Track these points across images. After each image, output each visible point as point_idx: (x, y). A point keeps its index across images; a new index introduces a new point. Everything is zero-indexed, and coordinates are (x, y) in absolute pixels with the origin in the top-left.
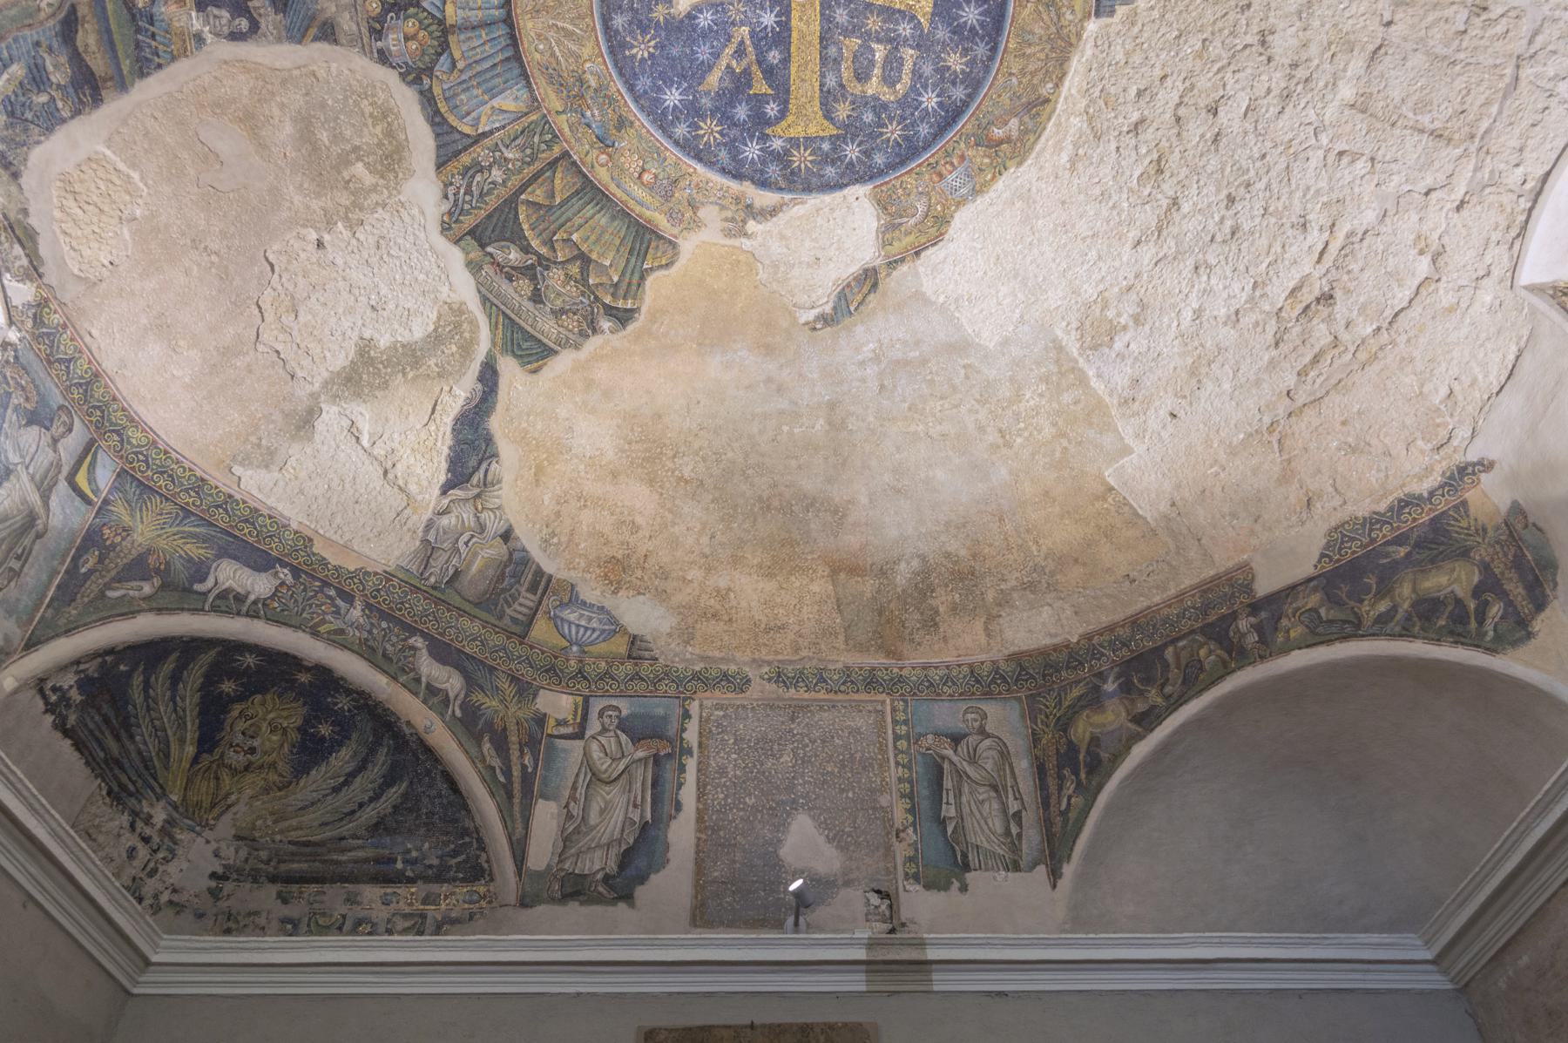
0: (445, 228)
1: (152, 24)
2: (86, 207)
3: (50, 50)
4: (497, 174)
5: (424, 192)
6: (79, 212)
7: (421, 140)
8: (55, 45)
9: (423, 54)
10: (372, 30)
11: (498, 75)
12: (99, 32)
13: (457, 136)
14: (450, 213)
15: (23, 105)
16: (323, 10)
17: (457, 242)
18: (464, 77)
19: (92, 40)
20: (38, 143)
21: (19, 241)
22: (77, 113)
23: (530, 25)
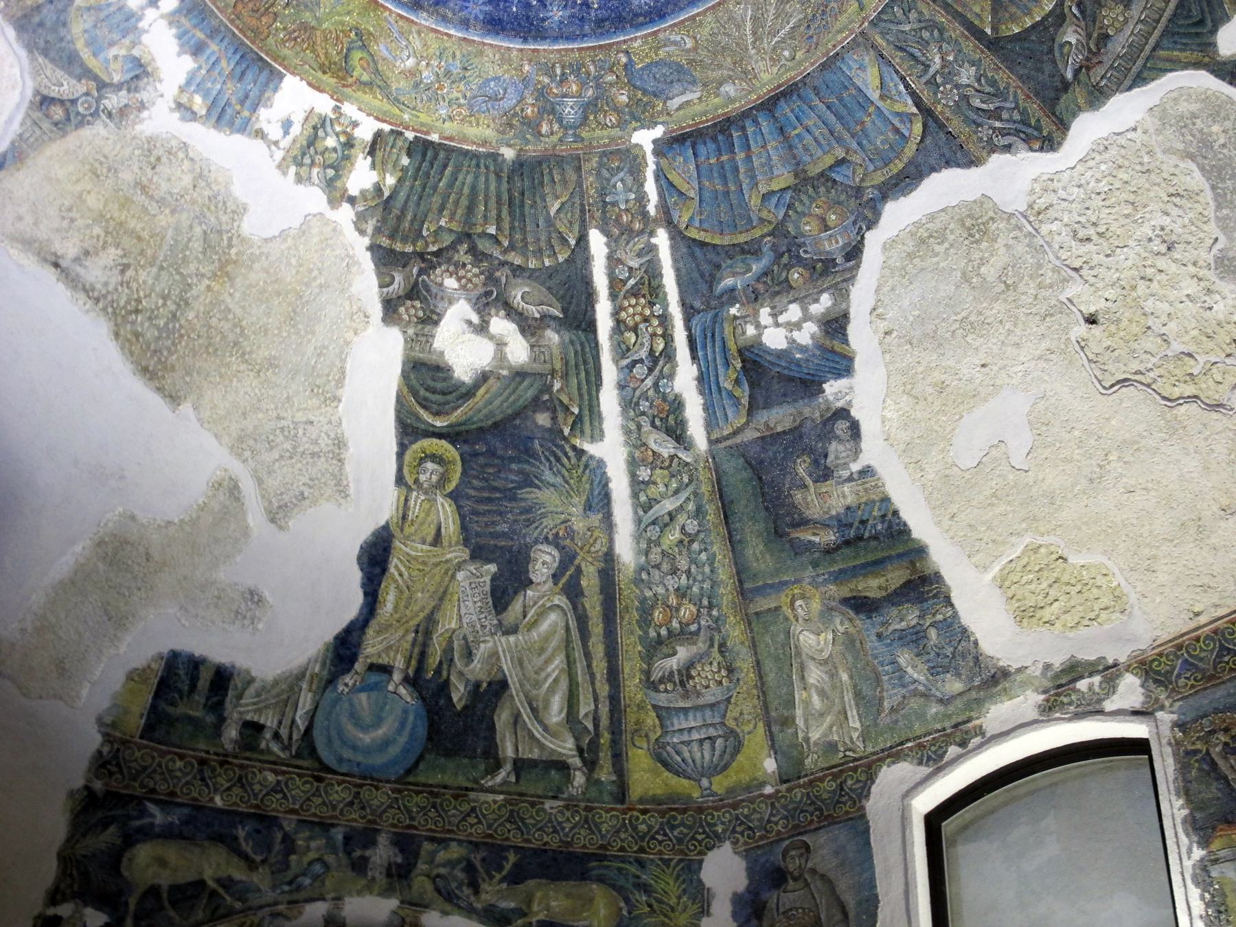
0: (1049, 143)
1: (851, 525)
2: (1051, 598)
3: (885, 624)
4: (966, 75)
5: (1011, 176)
6: (1056, 604)
7: (945, 189)
8: (878, 619)
9: (839, 203)
10: (825, 272)
11: (841, 99)
12: (865, 576)
13: (928, 141)
14: (1027, 140)
15: (938, 655)
16: (813, 337)
17: (1063, 126)
18: (854, 145)
19: (874, 583)
20: (976, 643)
21: (1075, 680)
22: (948, 602)
23: (765, 77)
